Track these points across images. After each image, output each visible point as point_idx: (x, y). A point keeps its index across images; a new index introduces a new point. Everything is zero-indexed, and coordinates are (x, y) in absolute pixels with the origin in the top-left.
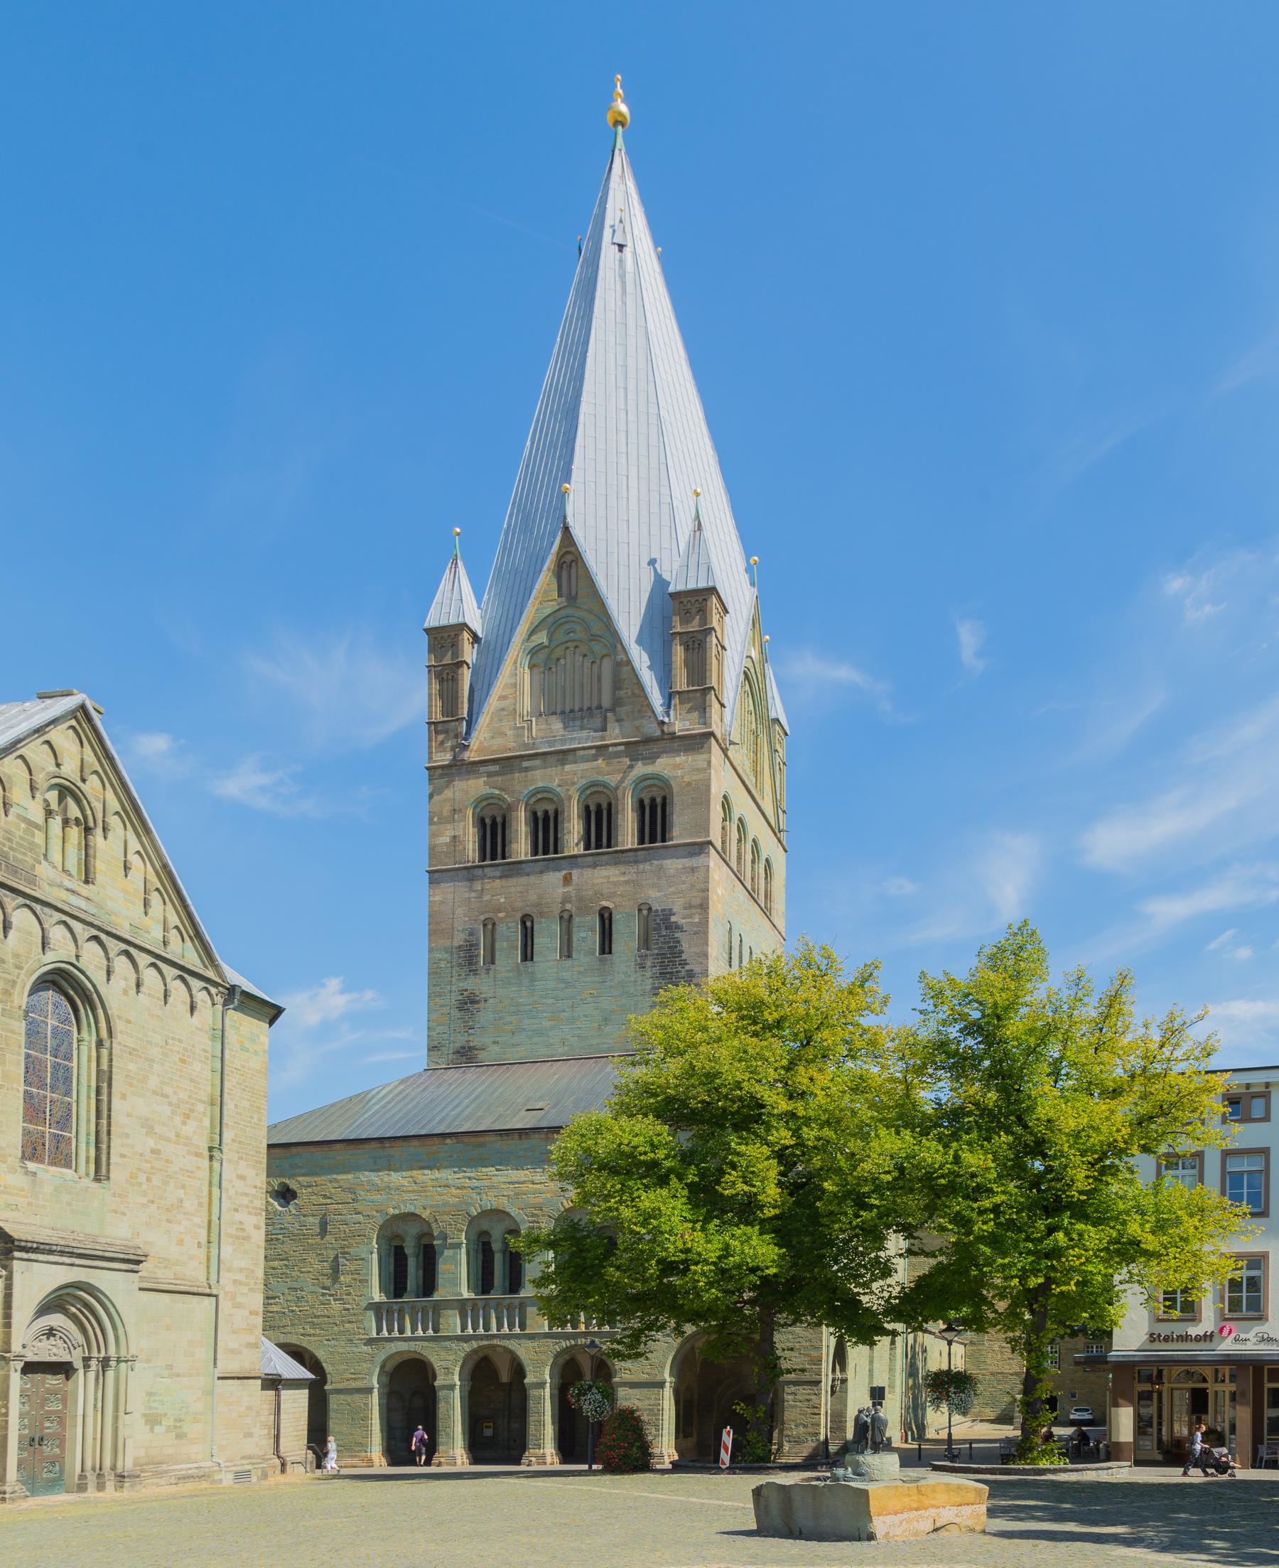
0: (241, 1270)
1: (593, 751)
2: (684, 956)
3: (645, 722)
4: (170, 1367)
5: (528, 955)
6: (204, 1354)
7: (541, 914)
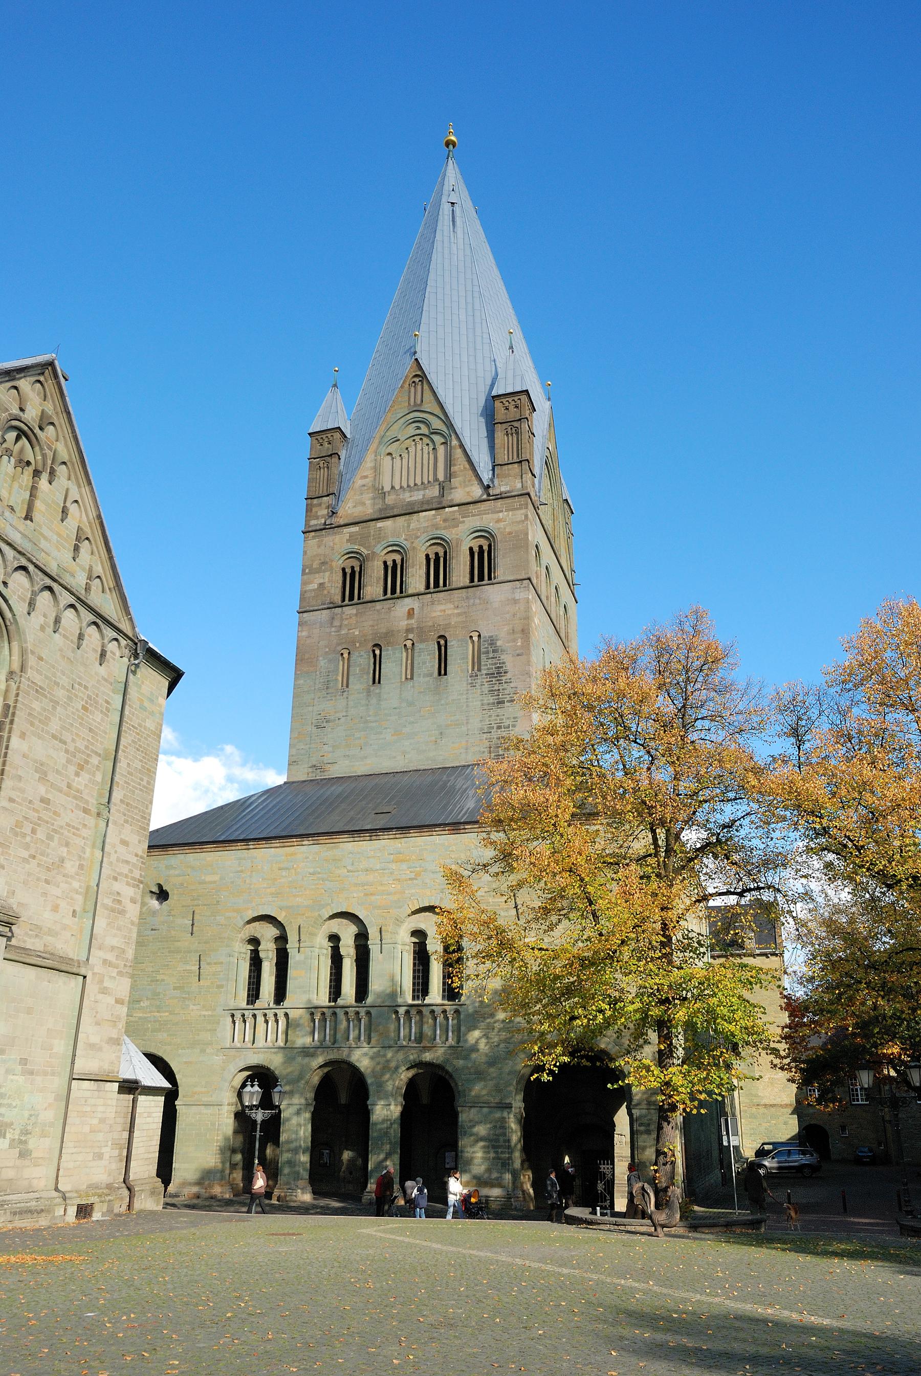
0: (113, 948)
1: (433, 512)
2: (509, 675)
4: (24, 1062)
5: (376, 679)
6: (61, 1047)
7: (388, 644)
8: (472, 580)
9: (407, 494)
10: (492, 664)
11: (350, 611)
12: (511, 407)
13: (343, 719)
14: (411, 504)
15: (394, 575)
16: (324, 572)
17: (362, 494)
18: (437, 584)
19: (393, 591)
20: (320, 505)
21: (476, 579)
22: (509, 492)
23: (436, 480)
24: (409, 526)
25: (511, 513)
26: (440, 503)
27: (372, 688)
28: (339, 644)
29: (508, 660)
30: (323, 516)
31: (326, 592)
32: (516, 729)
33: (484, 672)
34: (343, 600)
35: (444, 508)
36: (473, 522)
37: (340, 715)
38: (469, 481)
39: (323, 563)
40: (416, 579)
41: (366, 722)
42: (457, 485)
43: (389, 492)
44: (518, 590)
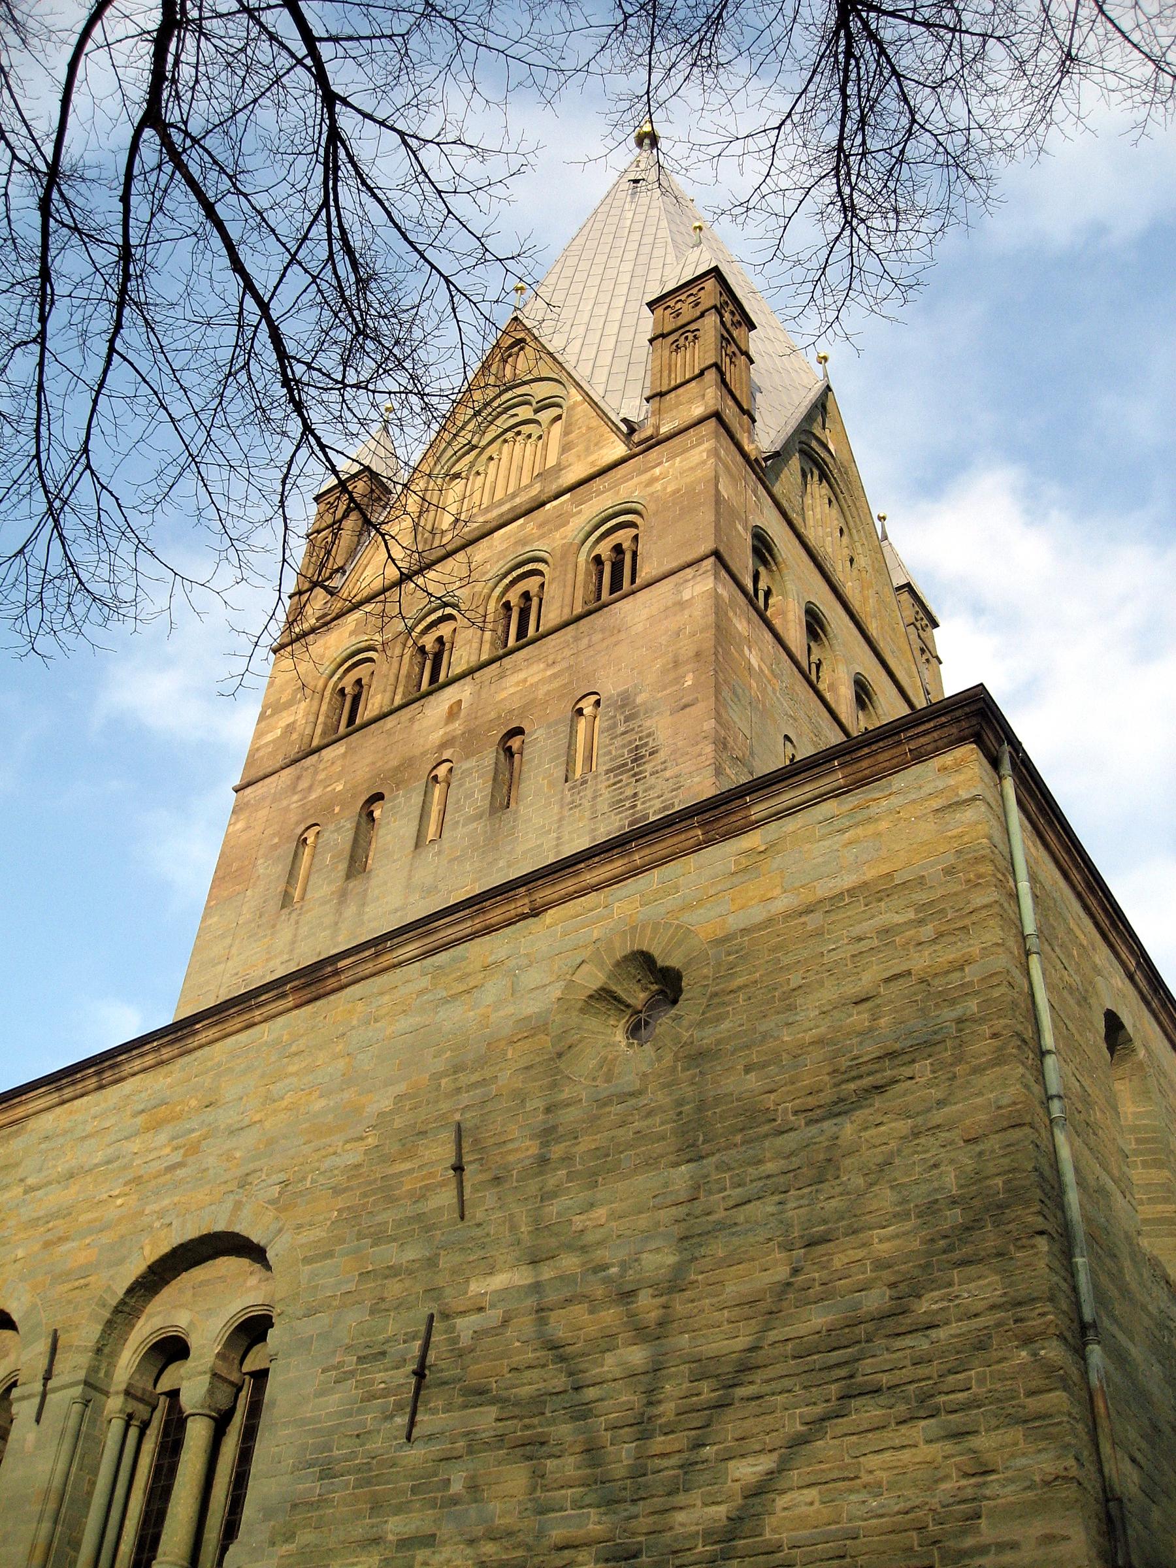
2: (662, 755)
10: (624, 746)
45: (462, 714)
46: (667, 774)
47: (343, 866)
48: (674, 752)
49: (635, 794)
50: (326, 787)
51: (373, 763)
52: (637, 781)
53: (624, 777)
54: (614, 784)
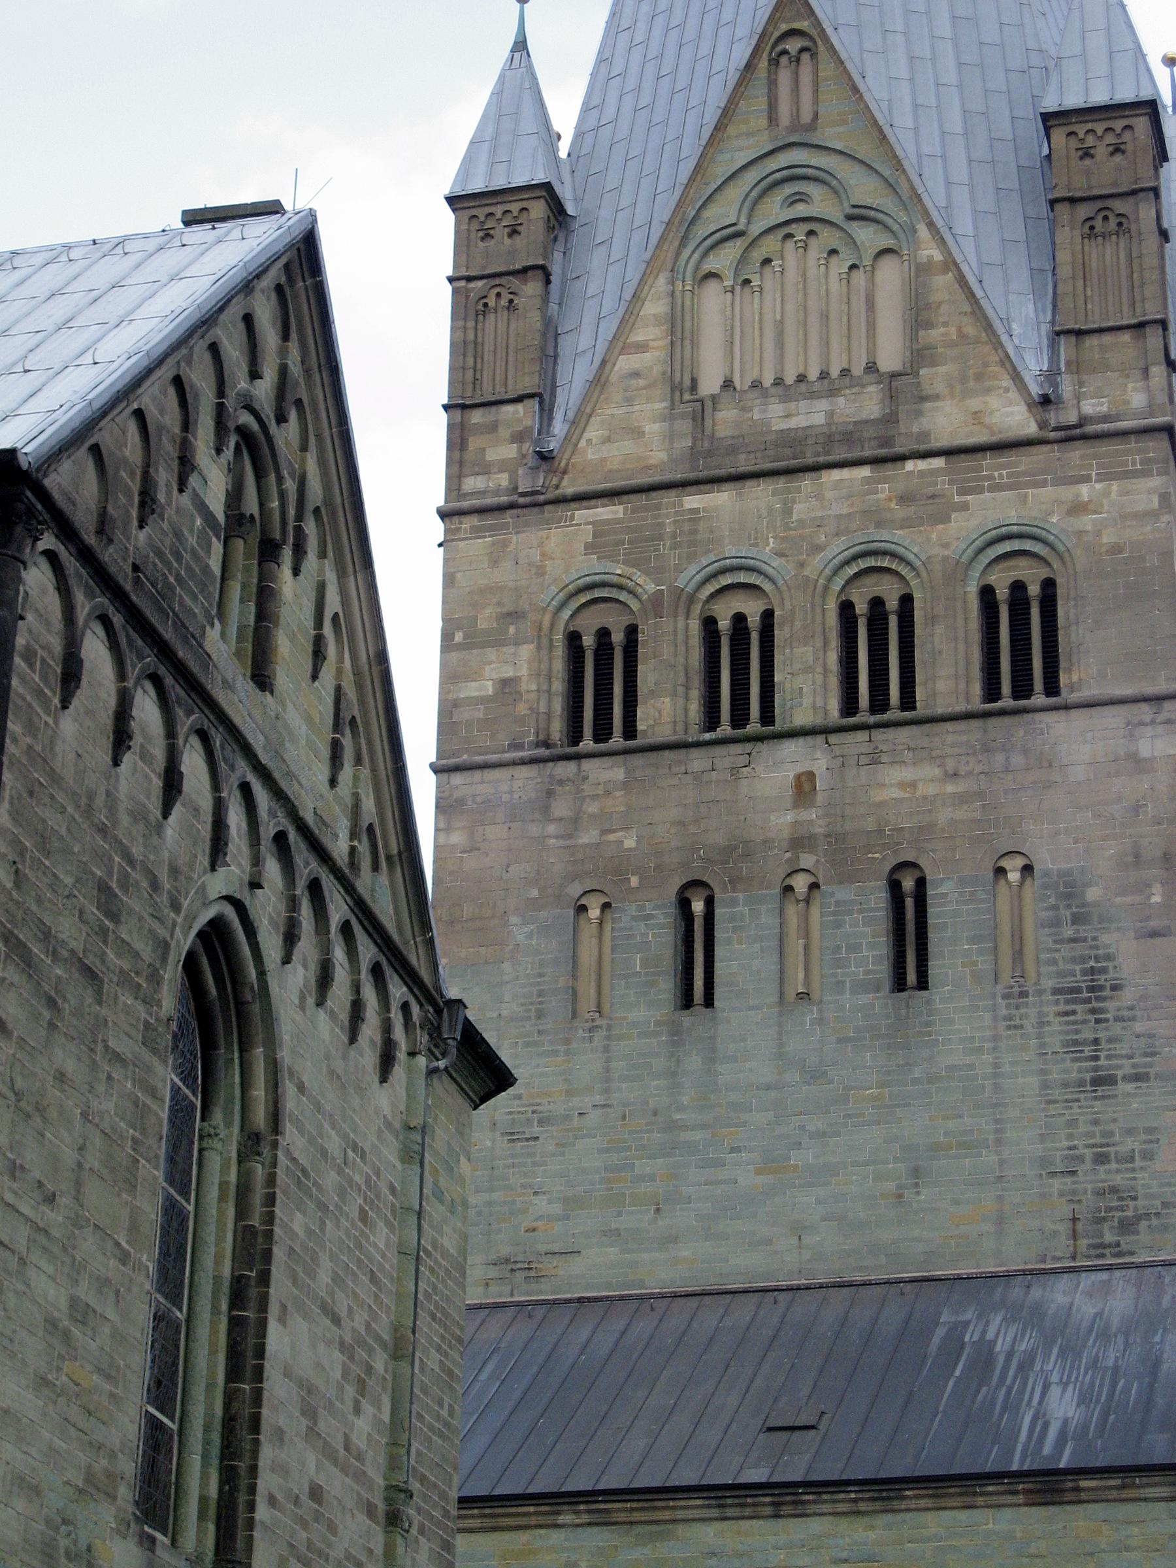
1: (865, 471)
2: (1128, 996)
3: (994, 402)
7: (735, 882)
8: (992, 692)
9: (776, 409)
10: (1073, 960)
11: (604, 773)
12: (1101, 151)
13: (594, 1117)
14: (792, 440)
15: (737, 668)
16: (517, 643)
17: (628, 401)
18: (879, 703)
19: (740, 717)
20: (493, 427)
21: (1006, 687)
22: (1106, 418)
23: (871, 368)
24: (787, 512)
25: (1115, 486)
26: (887, 442)
27: (687, 1019)
28: (575, 877)
29: (1125, 950)
30: (503, 466)
31: (522, 708)
32: (1158, 1166)
33: (1049, 983)
34: (575, 736)
35: (903, 458)
36: (990, 507)
37: (585, 1102)
38: (979, 377)
39: (514, 616)
40: (806, 679)
41: (673, 1127)
42: (940, 387)
43: (714, 398)
44: (1149, 731)
45: (820, 798)
46: (1138, 1027)
47: (667, 987)
48: (1144, 998)
49: (1096, 1041)
50: (605, 832)
51: (681, 823)
52: (1098, 1021)
53: (1079, 1008)
54: (1066, 1014)
